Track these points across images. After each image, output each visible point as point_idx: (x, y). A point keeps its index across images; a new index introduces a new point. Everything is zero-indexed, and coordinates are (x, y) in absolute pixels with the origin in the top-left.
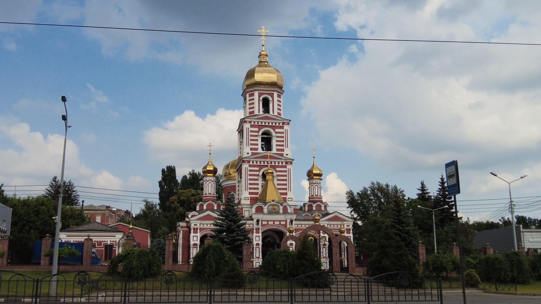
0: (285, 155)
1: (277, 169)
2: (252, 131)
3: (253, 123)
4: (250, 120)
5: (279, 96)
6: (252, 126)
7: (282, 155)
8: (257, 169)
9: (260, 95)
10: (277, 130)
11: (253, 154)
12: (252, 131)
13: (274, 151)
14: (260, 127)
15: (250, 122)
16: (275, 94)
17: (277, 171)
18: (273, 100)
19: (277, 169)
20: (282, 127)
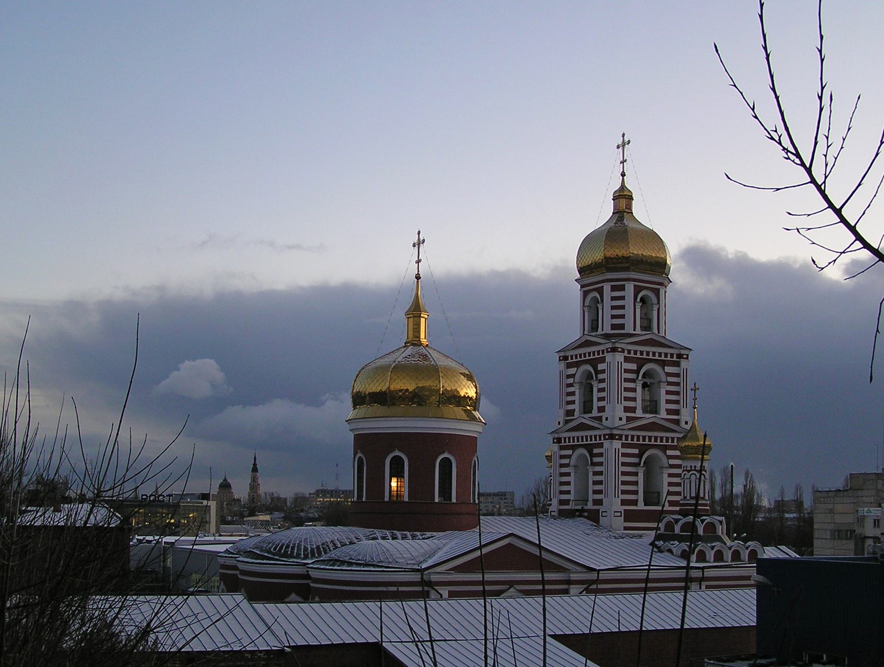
0: (604, 419)
1: (596, 451)
2: (569, 376)
3: (570, 361)
4: (562, 354)
5: (614, 288)
6: (569, 366)
7: (599, 419)
8: (569, 452)
9: (585, 294)
10: (601, 367)
11: (567, 422)
12: (569, 376)
13: (595, 413)
14: (577, 365)
15: (565, 358)
16: (607, 287)
17: (592, 455)
18: (602, 301)
19: (596, 451)
20: (603, 360)
